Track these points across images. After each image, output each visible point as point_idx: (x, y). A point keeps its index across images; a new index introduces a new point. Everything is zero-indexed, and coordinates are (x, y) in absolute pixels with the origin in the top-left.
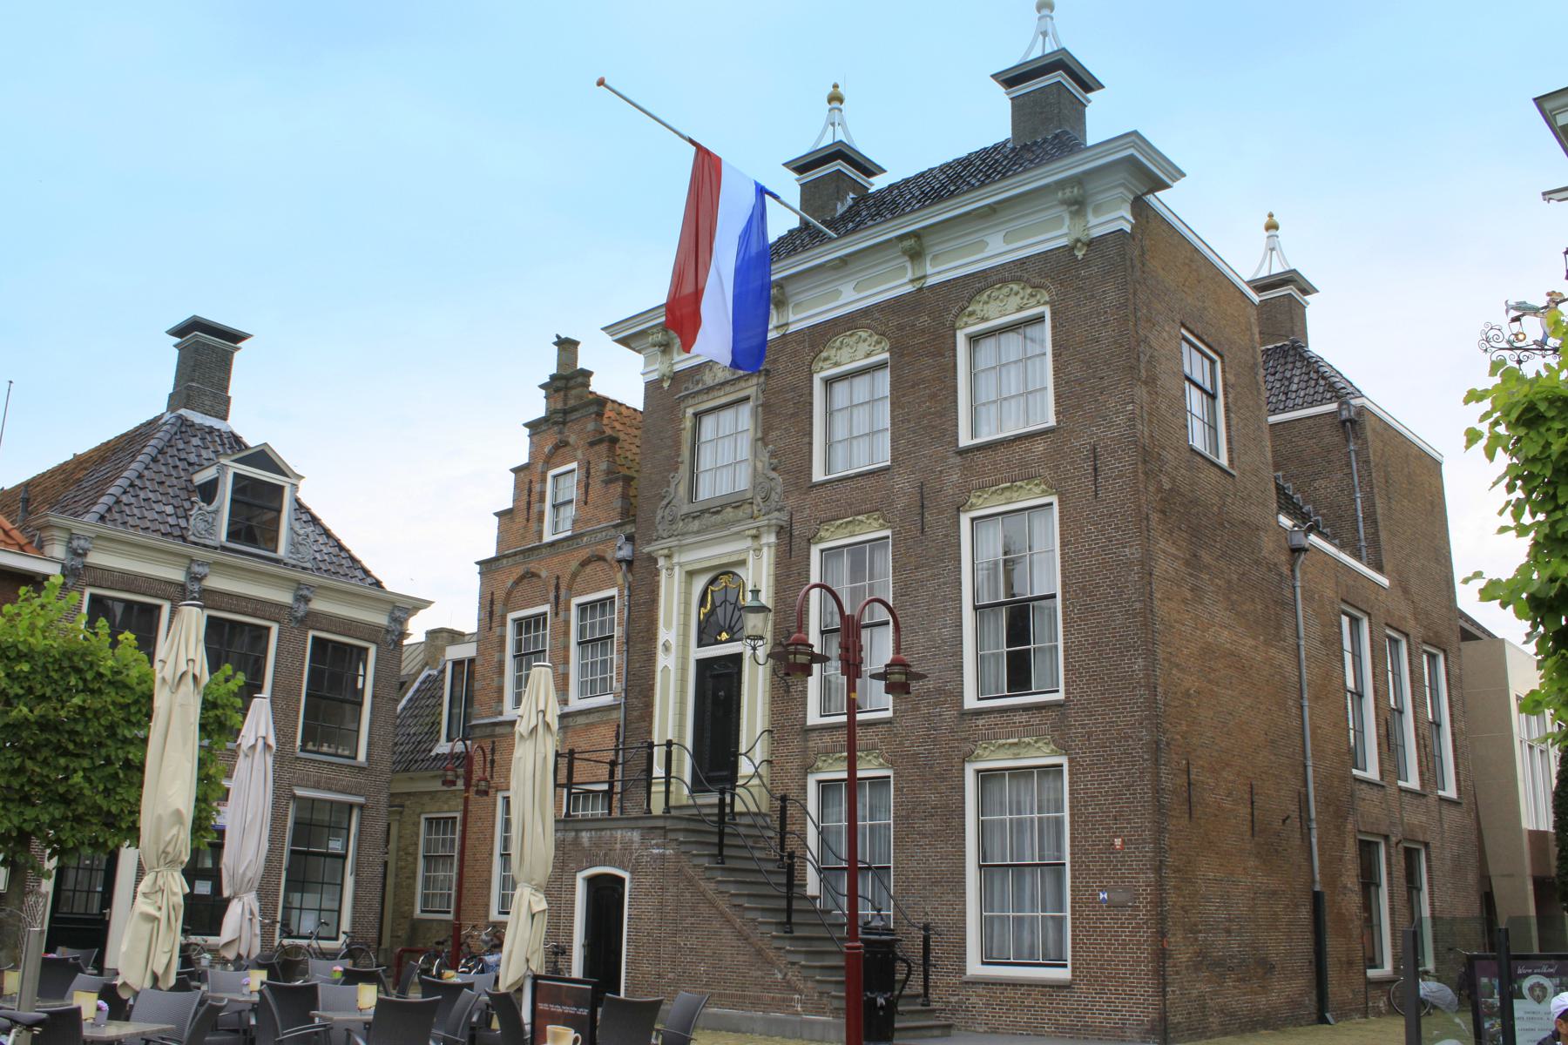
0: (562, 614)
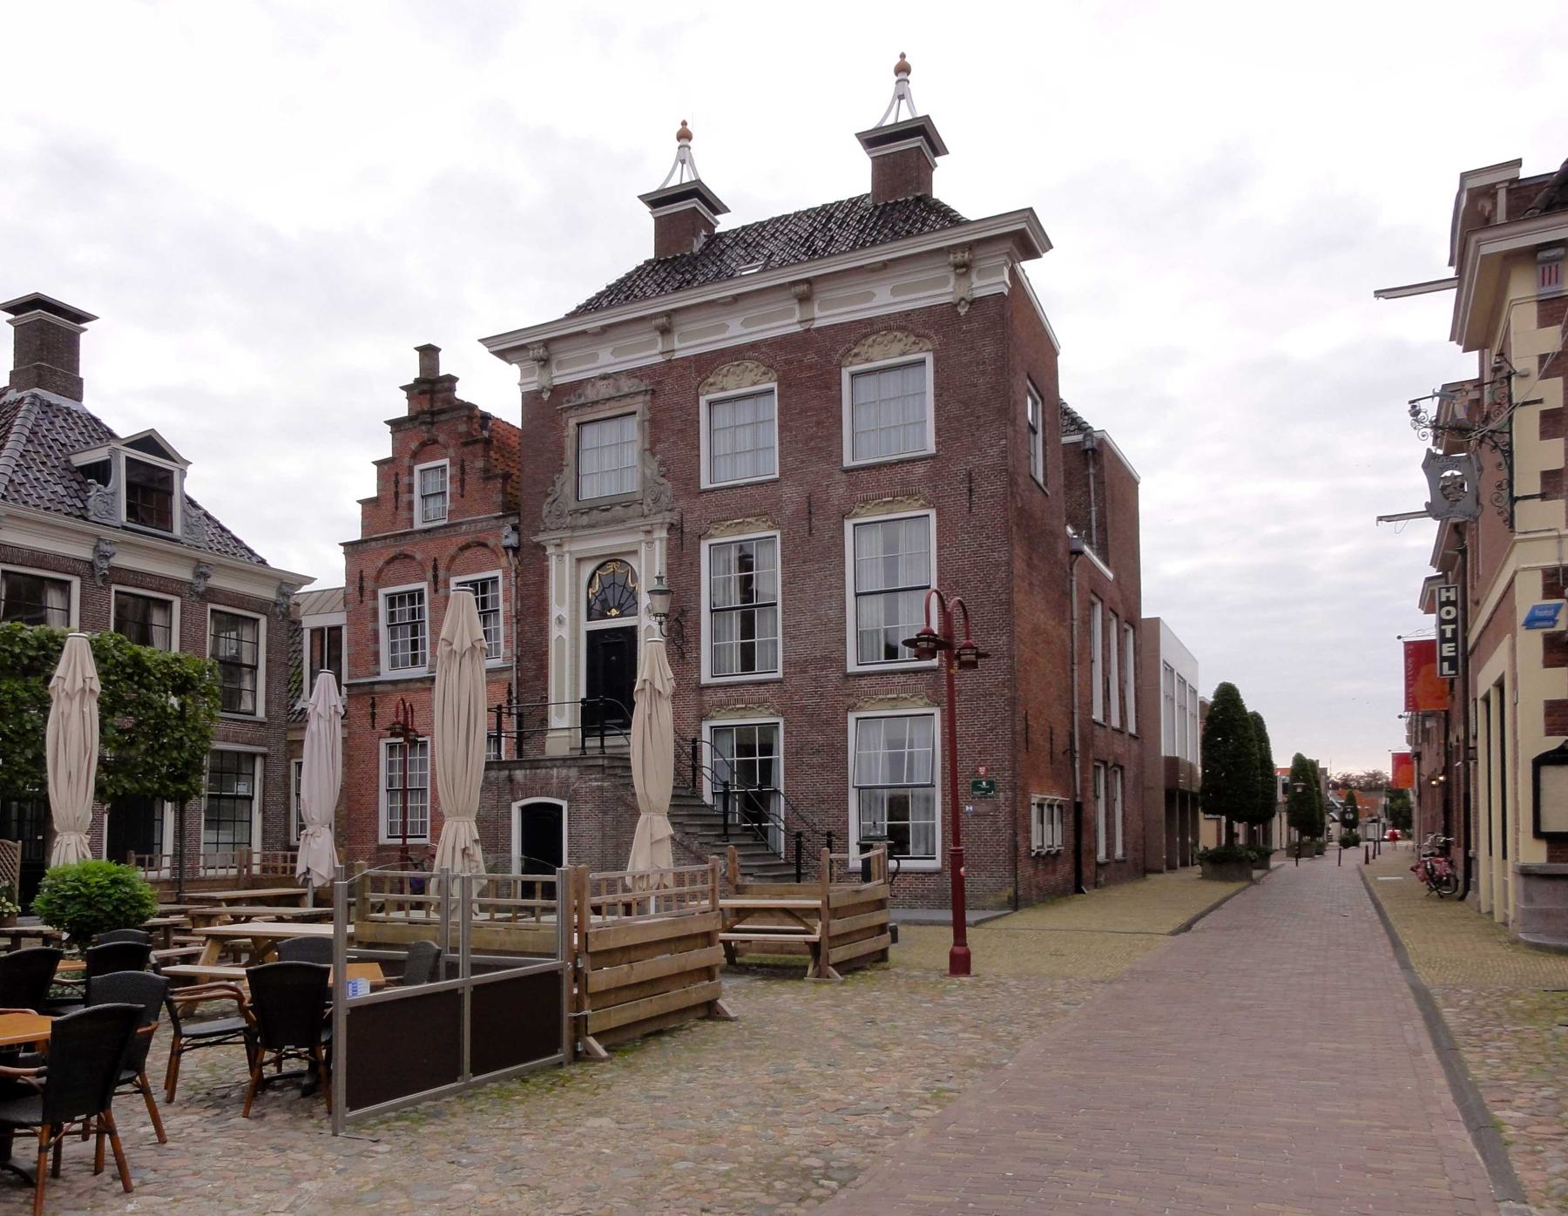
0: (442, 591)
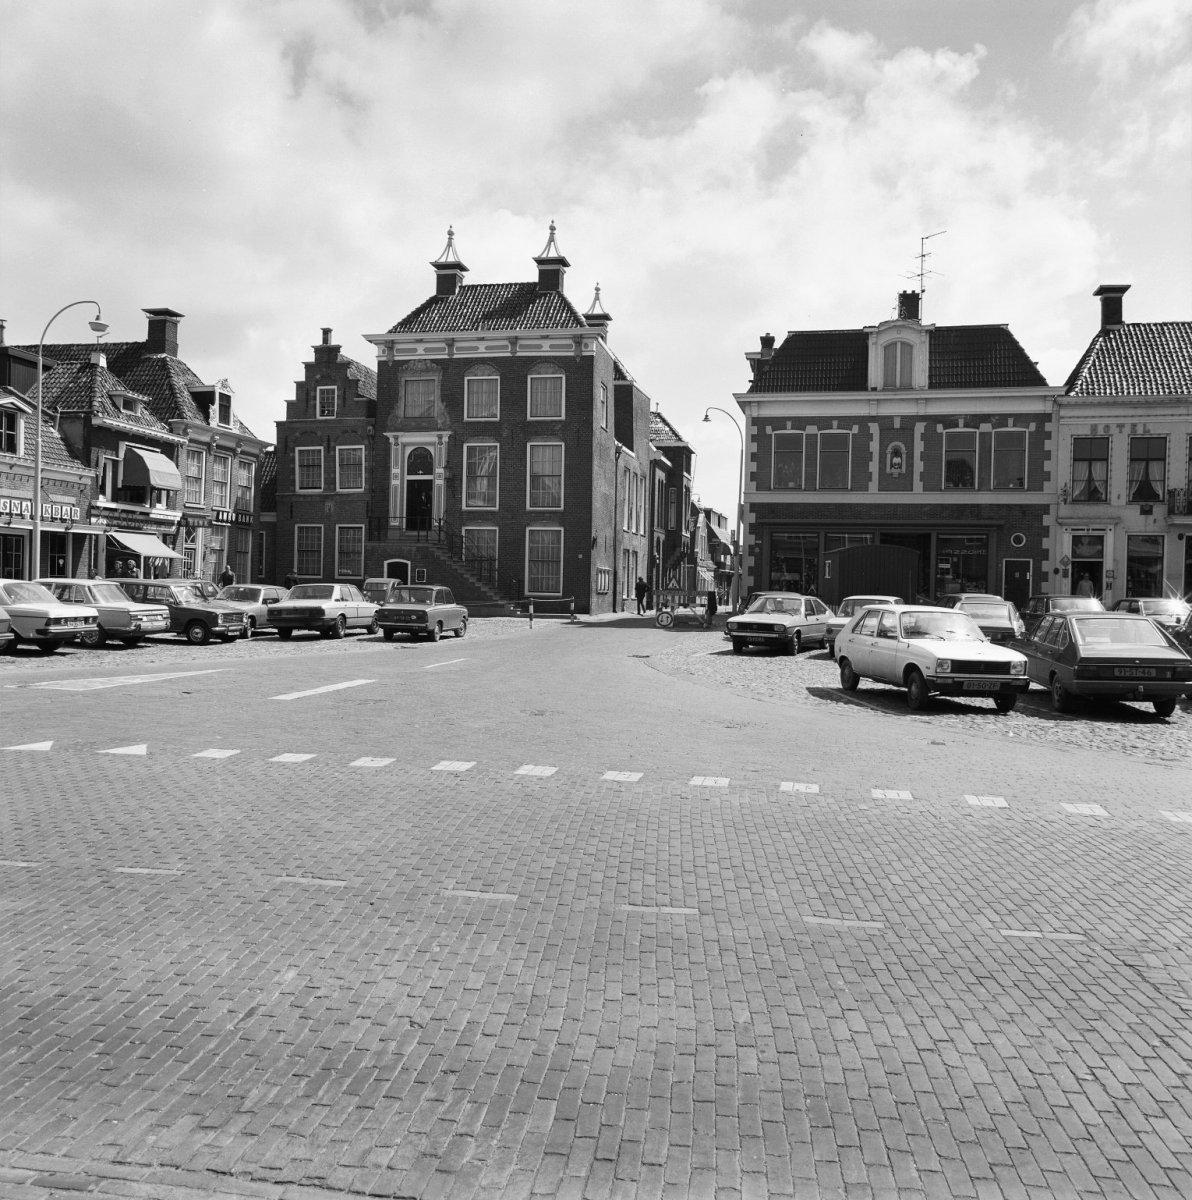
0: (332, 453)
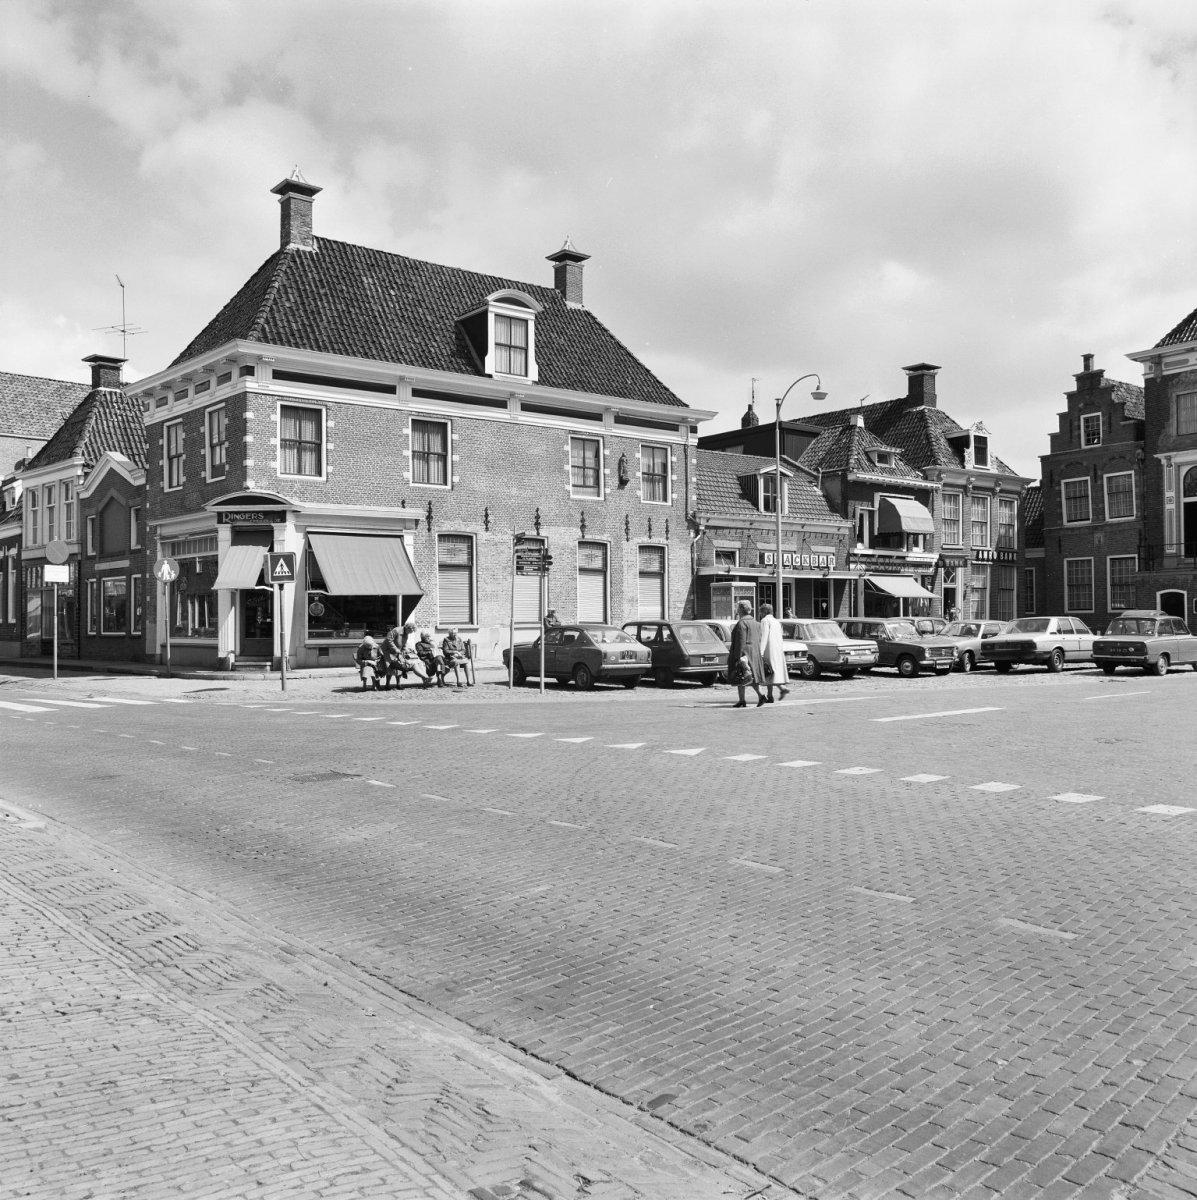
0: (1099, 483)
